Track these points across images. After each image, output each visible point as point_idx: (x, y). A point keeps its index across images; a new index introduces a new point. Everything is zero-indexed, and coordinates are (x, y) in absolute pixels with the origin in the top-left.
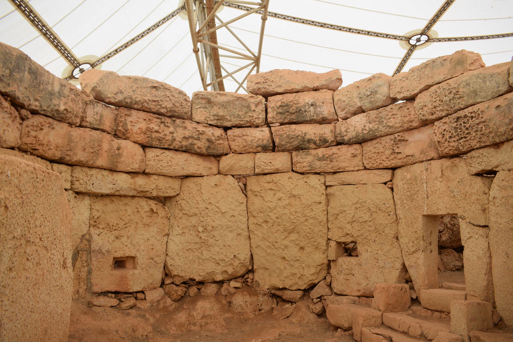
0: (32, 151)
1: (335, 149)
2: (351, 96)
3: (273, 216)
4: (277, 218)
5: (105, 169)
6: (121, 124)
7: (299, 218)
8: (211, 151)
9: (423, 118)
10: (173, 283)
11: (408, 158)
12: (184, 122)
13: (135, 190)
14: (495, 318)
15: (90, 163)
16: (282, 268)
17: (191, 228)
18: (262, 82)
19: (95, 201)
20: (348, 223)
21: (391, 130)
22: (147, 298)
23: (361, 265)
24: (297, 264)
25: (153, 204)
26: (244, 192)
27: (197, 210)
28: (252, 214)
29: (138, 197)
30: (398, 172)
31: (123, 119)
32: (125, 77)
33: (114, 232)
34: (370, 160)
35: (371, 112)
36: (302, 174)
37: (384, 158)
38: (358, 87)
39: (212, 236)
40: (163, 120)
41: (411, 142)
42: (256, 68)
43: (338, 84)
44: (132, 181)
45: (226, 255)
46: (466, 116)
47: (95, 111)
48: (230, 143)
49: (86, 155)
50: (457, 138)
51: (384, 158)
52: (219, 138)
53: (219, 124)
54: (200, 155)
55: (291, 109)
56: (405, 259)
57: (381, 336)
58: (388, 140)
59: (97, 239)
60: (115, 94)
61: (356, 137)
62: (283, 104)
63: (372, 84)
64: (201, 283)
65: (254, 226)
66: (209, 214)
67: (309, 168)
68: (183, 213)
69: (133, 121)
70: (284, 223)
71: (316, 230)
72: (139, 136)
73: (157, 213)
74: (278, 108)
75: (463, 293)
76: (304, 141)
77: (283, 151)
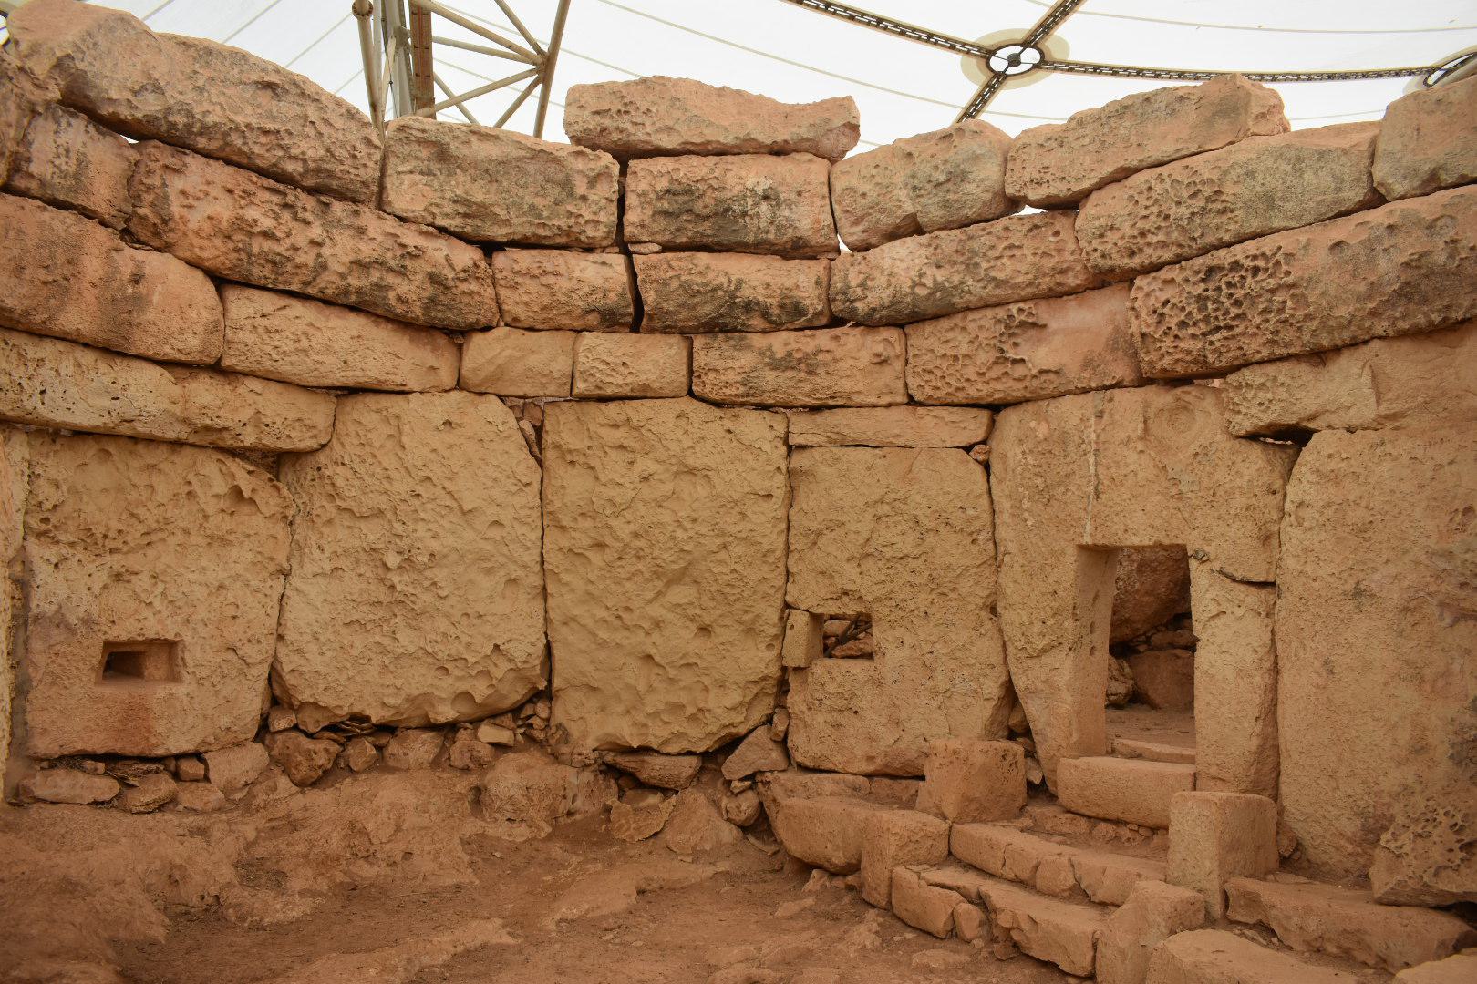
1: (823, 338)
2: (886, 182)
3: (624, 531)
4: (636, 535)
5: (86, 345)
6: (148, 198)
7: (702, 540)
8: (440, 315)
9: (1101, 262)
10: (296, 728)
11: (1044, 377)
12: (356, 213)
13: (185, 421)
14: (1285, 842)
15: (38, 318)
16: (642, 687)
17: (363, 556)
18: (614, 109)
19: (45, 450)
20: (848, 561)
21: (999, 292)
22: (211, 775)
23: (880, 684)
24: (687, 678)
25: (241, 473)
26: (536, 449)
27: (384, 498)
28: (557, 520)
29: (193, 445)
30: (1010, 419)
31: (156, 180)
32: (172, 38)
33: (108, 558)
34: (927, 377)
35: (943, 234)
36: (717, 404)
37: (970, 372)
38: (910, 154)
39: (427, 584)
40: (290, 199)
41: (1055, 333)
42: (538, 89)
43: (845, 140)
44: (177, 390)
45: (468, 645)
46: (1236, 266)
47: (60, 141)
48: (503, 293)
49: (23, 290)
50: (1203, 327)
51: (970, 372)
52: (469, 274)
53: (469, 230)
54: (404, 324)
55: (701, 204)
56: (1013, 670)
57: (955, 894)
58: (988, 323)
59: (50, 580)
60: (135, 93)
61: (892, 304)
62: (675, 186)
63: (953, 151)
64: (388, 729)
65: (560, 556)
66: (423, 515)
67: (742, 389)
68: (338, 507)
69: (191, 191)
70: (656, 553)
71: (753, 576)
72: (205, 243)
73: (252, 501)
74: (659, 198)
75: (1187, 769)
76: (733, 306)
77: (666, 331)
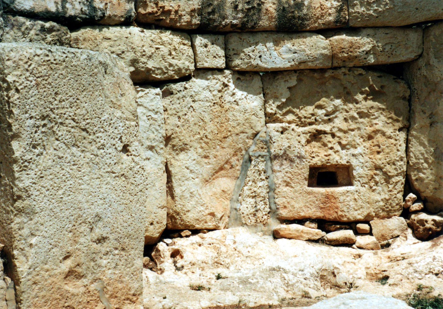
0: (156, 23)
22: (373, 232)
59: (279, 139)
